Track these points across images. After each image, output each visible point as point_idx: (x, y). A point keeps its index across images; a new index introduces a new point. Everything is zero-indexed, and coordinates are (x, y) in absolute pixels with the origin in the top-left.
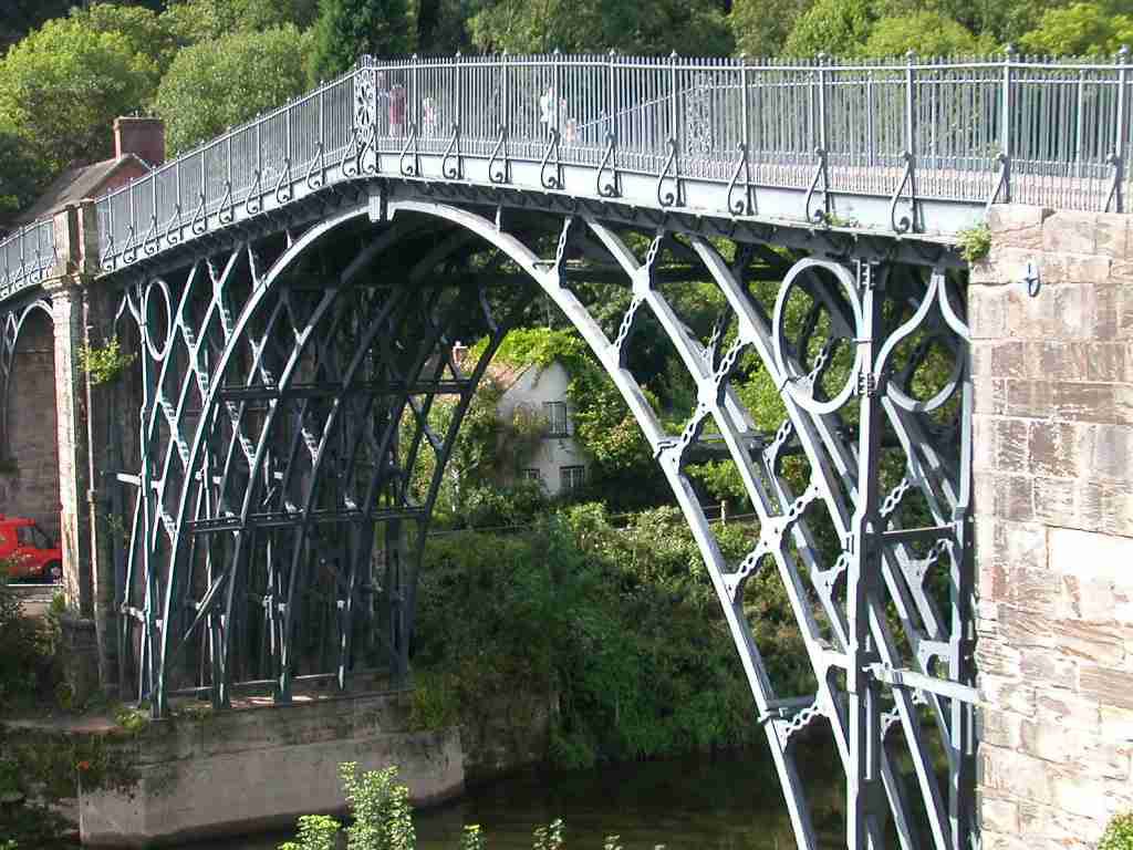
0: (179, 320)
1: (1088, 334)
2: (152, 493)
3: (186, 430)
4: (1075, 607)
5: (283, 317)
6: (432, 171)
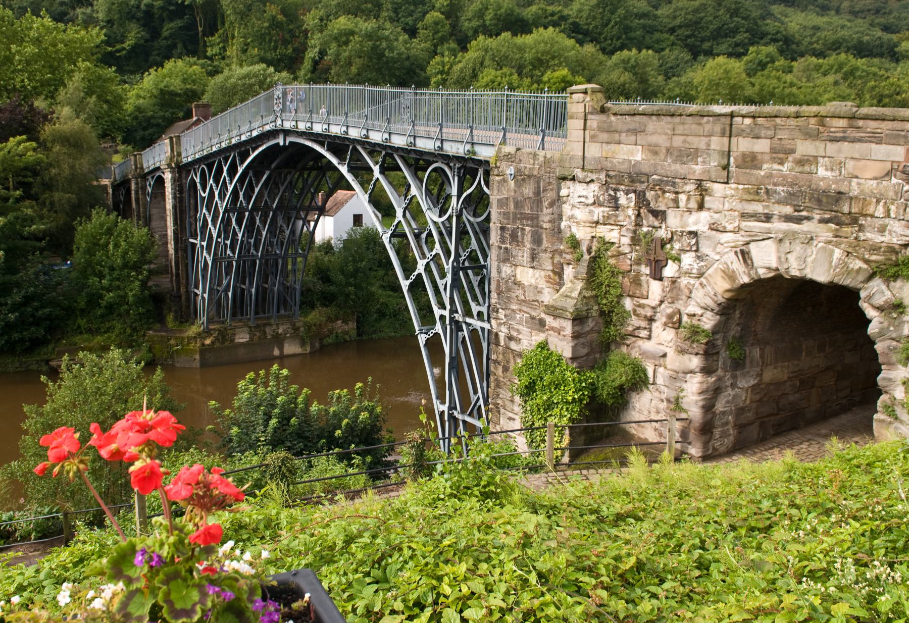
0: (211, 181)
1: (531, 195)
2: (202, 246)
4: (524, 295)
5: (250, 182)
6: (302, 126)
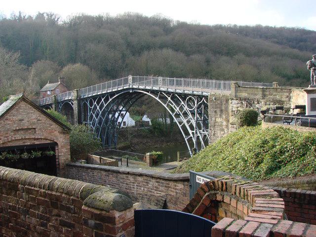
0: (95, 103)
3: (97, 116)
6: (141, 87)
